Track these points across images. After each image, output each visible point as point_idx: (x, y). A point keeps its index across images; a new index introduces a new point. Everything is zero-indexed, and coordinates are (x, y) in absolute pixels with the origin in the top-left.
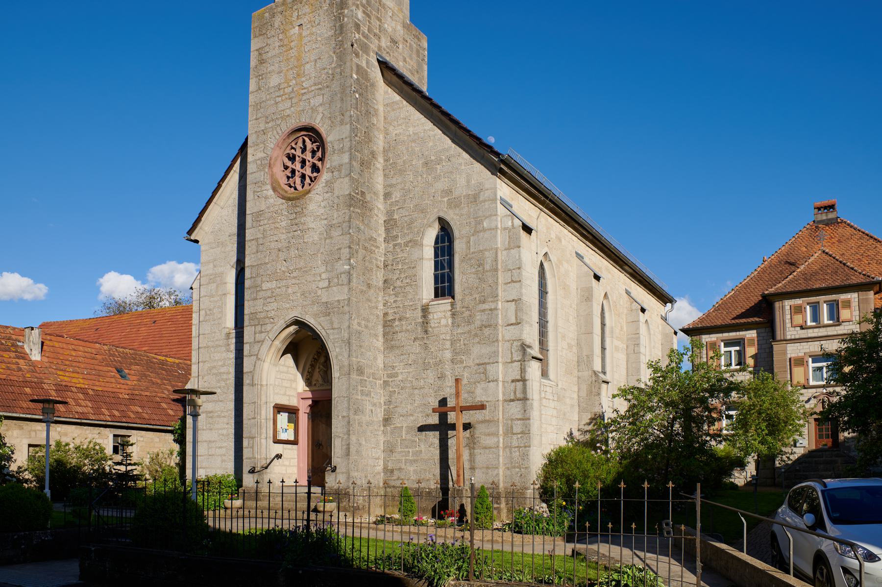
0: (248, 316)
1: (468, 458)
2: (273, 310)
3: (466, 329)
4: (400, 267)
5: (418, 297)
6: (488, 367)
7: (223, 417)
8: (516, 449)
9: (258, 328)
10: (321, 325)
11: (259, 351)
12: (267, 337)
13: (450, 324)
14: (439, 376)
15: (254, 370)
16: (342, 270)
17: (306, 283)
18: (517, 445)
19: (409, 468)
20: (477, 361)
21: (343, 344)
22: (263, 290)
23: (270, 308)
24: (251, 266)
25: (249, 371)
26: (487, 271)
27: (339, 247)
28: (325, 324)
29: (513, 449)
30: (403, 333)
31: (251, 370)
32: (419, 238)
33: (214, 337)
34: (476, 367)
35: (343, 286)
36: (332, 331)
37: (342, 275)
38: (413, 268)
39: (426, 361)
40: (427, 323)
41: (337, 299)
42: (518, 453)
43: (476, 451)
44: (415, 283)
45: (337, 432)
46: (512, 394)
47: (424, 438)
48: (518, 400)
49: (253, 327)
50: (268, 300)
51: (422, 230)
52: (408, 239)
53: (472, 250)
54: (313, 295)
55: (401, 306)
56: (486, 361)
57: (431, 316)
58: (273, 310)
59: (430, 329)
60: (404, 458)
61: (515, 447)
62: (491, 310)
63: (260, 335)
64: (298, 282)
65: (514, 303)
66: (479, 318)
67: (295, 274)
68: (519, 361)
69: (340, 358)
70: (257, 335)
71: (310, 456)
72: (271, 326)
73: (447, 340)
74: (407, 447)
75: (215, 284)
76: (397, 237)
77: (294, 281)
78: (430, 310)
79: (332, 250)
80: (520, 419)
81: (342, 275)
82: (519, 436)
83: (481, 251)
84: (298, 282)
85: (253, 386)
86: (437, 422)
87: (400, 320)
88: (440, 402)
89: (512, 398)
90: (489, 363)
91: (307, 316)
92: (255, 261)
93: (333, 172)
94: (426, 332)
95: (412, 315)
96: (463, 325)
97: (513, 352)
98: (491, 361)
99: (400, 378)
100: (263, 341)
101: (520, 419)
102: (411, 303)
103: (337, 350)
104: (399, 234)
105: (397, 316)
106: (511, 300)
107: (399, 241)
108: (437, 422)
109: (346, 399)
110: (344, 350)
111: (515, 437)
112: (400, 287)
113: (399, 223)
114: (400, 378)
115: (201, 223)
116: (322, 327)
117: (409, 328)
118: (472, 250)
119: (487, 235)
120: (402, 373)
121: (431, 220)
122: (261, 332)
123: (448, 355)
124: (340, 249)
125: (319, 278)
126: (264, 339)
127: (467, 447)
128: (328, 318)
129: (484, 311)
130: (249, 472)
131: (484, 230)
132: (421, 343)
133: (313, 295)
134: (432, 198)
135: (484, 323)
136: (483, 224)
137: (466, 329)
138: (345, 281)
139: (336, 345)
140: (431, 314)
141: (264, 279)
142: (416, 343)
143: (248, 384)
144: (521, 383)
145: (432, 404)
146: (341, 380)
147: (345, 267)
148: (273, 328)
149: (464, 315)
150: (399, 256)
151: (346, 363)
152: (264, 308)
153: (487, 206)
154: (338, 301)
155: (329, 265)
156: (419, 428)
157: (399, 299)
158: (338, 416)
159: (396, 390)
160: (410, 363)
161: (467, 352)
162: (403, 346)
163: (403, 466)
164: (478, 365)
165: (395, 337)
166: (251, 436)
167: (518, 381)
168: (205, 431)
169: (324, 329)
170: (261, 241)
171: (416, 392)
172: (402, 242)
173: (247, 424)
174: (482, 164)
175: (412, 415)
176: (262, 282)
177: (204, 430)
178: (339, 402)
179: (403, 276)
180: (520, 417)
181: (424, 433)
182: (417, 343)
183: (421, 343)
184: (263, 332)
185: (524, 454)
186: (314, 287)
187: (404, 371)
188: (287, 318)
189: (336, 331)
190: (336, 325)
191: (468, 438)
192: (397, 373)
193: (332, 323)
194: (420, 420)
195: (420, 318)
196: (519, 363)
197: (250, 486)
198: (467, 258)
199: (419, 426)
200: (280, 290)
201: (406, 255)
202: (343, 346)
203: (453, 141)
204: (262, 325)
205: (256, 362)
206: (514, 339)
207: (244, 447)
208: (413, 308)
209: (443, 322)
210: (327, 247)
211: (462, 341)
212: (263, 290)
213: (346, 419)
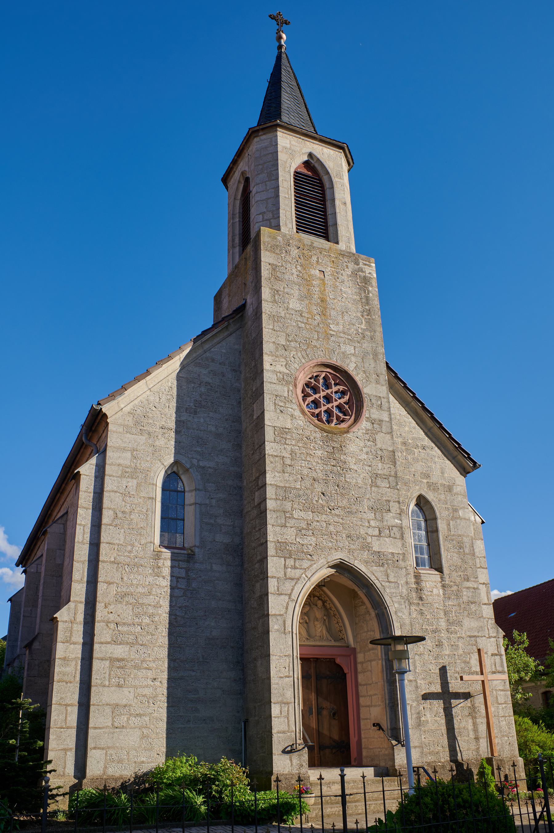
0: (273, 544)
1: (472, 727)
2: (311, 545)
3: (455, 602)
5: (410, 563)
6: (478, 639)
8: (503, 718)
9: (290, 562)
10: (374, 575)
11: (292, 590)
12: (304, 575)
13: (442, 595)
14: (437, 643)
15: (286, 613)
16: (394, 524)
17: (352, 525)
18: (503, 715)
20: (468, 634)
21: (403, 601)
22: (295, 519)
23: (306, 542)
24: (276, 486)
25: (278, 613)
26: (467, 554)
28: (382, 577)
29: (501, 719)
31: (282, 613)
32: (405, 508)
34: (469, 638)
36: (387, 584)
39: (424, 627)
40: (421, 590)
41: (390, 551)
42: (504, 722)
43: (478, 720)
46: (493, 666)
47: (429, 706)
48: (499, 672)
49: (283, 559)
50: (303, 532)
51: (407, 501)
53: (452, 533)
54: (361, 540)
56: (476, 634)
57: (423, 584)
58: (311, 545)
59: (424, 596)
61: (502, 717)
62: (474, 588)
63: (293, 571)
64: (341, 521)
65: (484, 585)
66: (466, 595)
67: (336, 512)
68: (495, 637)
69: (400, 614)
70: (289, 570)
72: (309, 563)
73: (441, 609)
77: (336, 519)
78: (422, 578)
79: (380, 500)
80: (502, 690)
82: (504, 705)
83: (460, 536)
84: (341, 521)
85: (285, 633)
86: (440, 690)
88: (440, 669)
89: (494, 670)
90: (478, 636)
91: (356, 561)
92: (281, 481)
93: (373, 424)
94: (421, 599)
96: (453, 597)
97: (489, 628)
98: (480, 634)
100: (298, 579)
101: (502, 690)
106: (482, 582)
108: (440, 690)
110: (403, 606)
111: (500, 707)
116: (376, 577)
118: (452, 533)
119: (463, 523)
121: (414, 495)
122: (295, 568)
123: (443, 624)
124: (389, 501)
125: (367, 524)
126: (300, 577)
127: (470, 717)
128: (382, 569)
129: (468, 588)
130: (284, 752)
131: (460, 518)
133: (361, 540)
134: (412, 476)
135: (470, 599)
136: (459, 513)
137: (455, 602)
139: (394, 599)
140: (424, 582)
141: (295, 506)
143: (278, 630)
144: (499, 657)
147: (396, 521)
148: (311, 566)
149: (452, 589)
151: (407, 621)
152: (298, 540)
153: (459, 499)
155: (377, 514)
156: (423, 696)
161: (459, 623)
164: (470, 637)
166: (285, 701)
167: (496, 655)
169: (378, 580)
170: (288, 462)
173: (278, 684)
174: (452, 463)
176: (293, 509)
180: (502, 688)
181: (428, 701)
184: (297, 568)
185: (509, 723)
186: (362, 532)
189: (393, 585)
190: (392, 579)
191: (470, 707)
193: (388, 576)
194: (423, 688)
195: (413, 584)
196: (495, 639)
197: (286, 772)
198: (449, 538)
199: (423, 693)
200: (318, 524)
202: (403, 603)
203: (426, 434)
205: (288, 604)
206: (488, 617)
207: (273, 716)
209: (435, 591)
210: (373, 494)
211: (453, 612)
212: (295, 519)
213: (414, 684)
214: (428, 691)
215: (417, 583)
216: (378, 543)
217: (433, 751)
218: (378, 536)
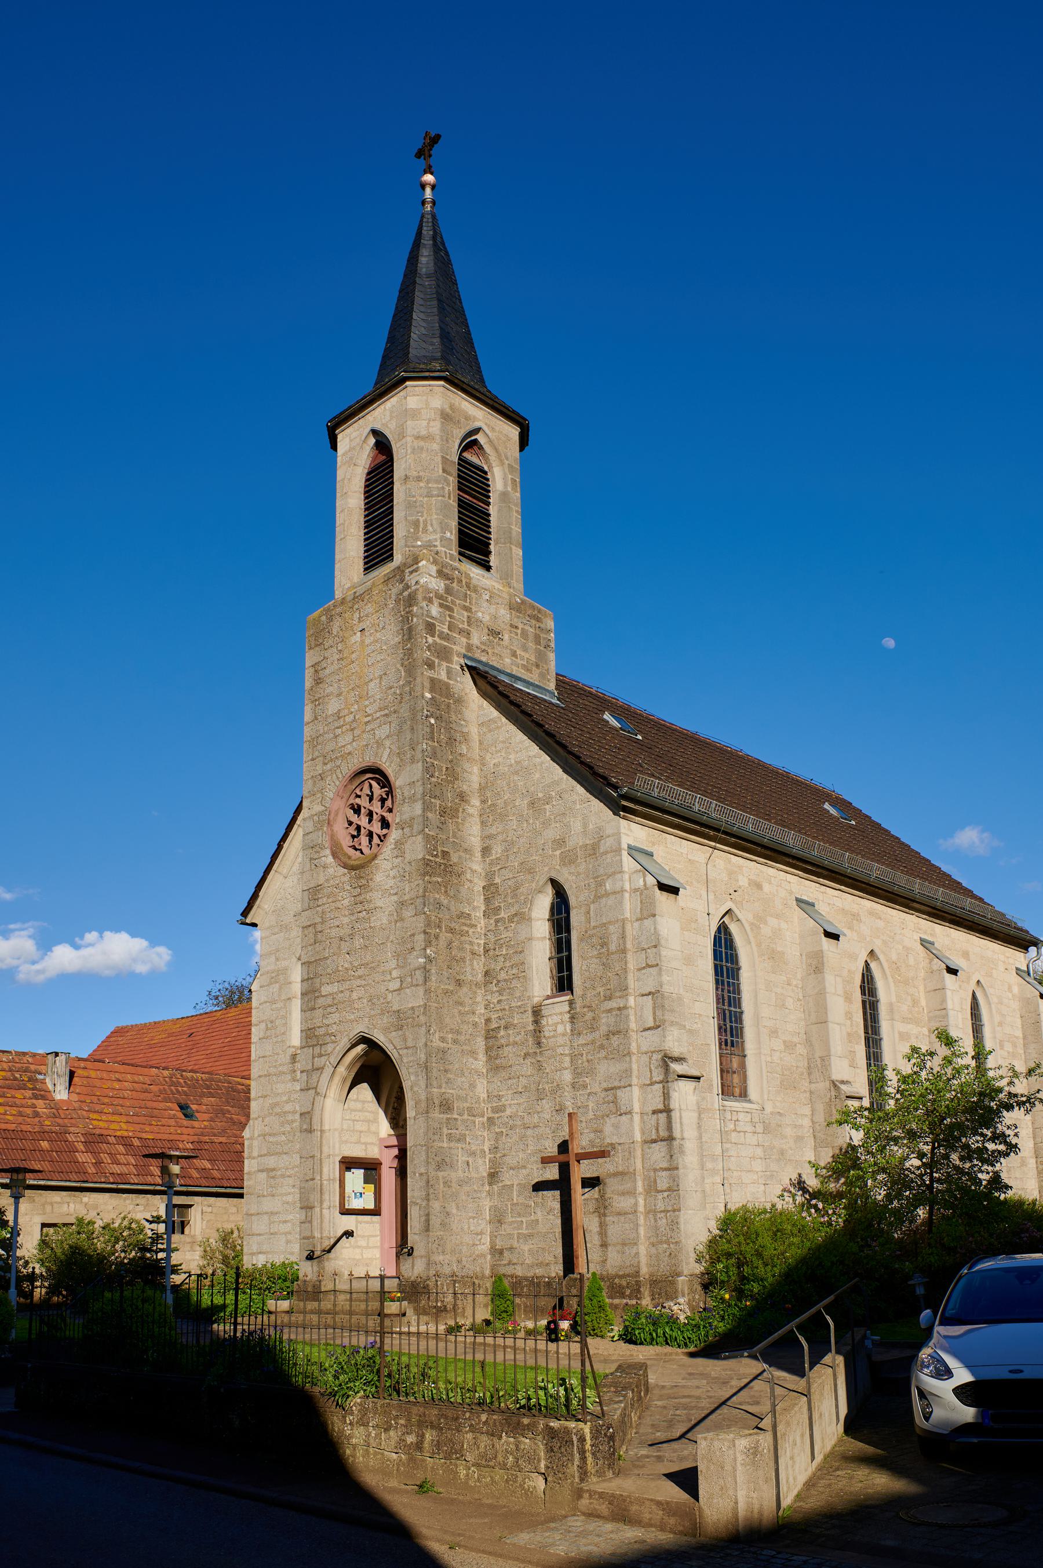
1: (598, 1229)
2: (335, 1023)
3: (590, 1037)
4: (504, 952)
5: (528, 994)
6: (619, 1093)
7: (289, 1176)
8: (662, 1215)
9: (317, 1050)
11: (318, 1082)
13: (569, 1031)
14: (557, 1108)
18: (663, 1209)
19: (523, 1247)
20: (605, 1085)
23: (331, 1021)
26: (612, 953)
27: (412, 932)
28: (399, 1044)
29: (659, 1215)
30: (511, 1047)
32: (527, 910)
33: (276, 1061)
34: (604, 1093)
35: (418, 988)
36: (405, 1051)
37: (417, 972)
38: (521, 952)
39: (540, 1087)
41: (410, 1005)
42: (664, 1221)
43: (608, 1219)
44: (523, 974)
45: (413, 1197)
46: (654, 1131)
47: (540, 1200)
48: (661, 1140)
50: (329, 1010)
52: (513, 911)
53: (593, 924)
55: (507, 1007)
56: (617, 1084)
57: (544, 1022)
58: (335, 1023)
60: (516, 1232)
61: (661, 1212)
62: (619, 1009)
63: (319, 1059)
64: (363, 983)
65: (650, 997)
66: (606, 1021)
67: (360, 972)
68: (661, 1082)
70: (316, 1059)
71: (399, 1232)
73: (566, 1055)
74: (519, 1215)
75: (277, 985)
76: (499, 909)
77: (359, 982)
78: (543, 1012)
80: (666, 1169)
81: (417, 972)
82: (666, 1194)
83: (604, 925)
84: (363, 983)
85: (311, 1132)
86: (557, 1177)
87: (506, 1028)
88: (559, 1146)
89: (654, 1137)
90: (620, 1087)
93: (403, 829)
95: (521, 1021)
96: (585, 1032)
97: (653, 1068)
98: (622, 1084)
99: (508, 1112)
100: (323, 1068)
101: (666, 1169)
102: (519, 1004)
103: (413, 1078)
104: (502, 905)
105: (503, 1023)
106: (647, 992)
107: (502, 915)
108: (557, 1177)
109: (424, 1148)
110: (420, 1077)
111: (660, 1196)
112: (505, 980)
113: (501, 889)
114: (508, 1112)
115: (259, 899)
117: (517, 1039)
118: (593, 924)
119: (611, 901)
120: (510, 1105)
121: (541, 883)
122: (321, 1055)
123: (567, 1076)
124: (413, 935)
127: (596, 1214)
128: (400, 1033)
129: (610, 1011)
131: (607, 894)
132: (533, 1060)
134: (541, 851)
135: (611, 1028)
136: (605, 886)
137: (590, 1037)
138: (421, 980)
140: (545, 1019)
141: (323, 980)
142: (526, 1060)
144: (665, 1114)
145: (550, 1150)
146: (417, 1121)
148: (334, 1049)
149: (586, 1018)
150: (503, 936)
151: (423, 1097)
153: (609, 860)
154: (413, 1008)
157: (504, 998)
158: (415, 1174)
159: (504, 1130)
160: (520, 1090)
161: (591, 1072)
162: (510, 1066)
163: (515, 1245)
164: (606, 1090)
165: (500, 1053)
167: (661, 1111)
168: (265, 1198)
169: (395, 1048)
170: (319, 928)
171: (529, 1132)
172: (506, 916)
174: (601, 801)
175: (524, 1167)
176: (322, 984)
177: (264, 1196)
178: (416, 1152)
179: (508, 964)
180: (665, 1165)
181: (541, 1193)
182: (528, 1061)
183: (533, 1060)
185: (672, 1221)
187: (513, 1102)
188: (351, 1036)
189: (410, 1051)
191: (597, 1199)
192: (504, 1106)
193: (405, 1040)
196: (661, 1085)
198: (587, 935)
199: (533, 1182)
201: (511, 935)
204: (321, 1045)
206: (653, 1049)
208: (522, 1010)
209: (560, 1029)
210: (397, 932)
211: (585, 1055)
213: (425, 1178)
214: (540, 1179)
215: (536, 1022)
216: (398, 999)
217: (542, 1263)
218: (399, 990)
